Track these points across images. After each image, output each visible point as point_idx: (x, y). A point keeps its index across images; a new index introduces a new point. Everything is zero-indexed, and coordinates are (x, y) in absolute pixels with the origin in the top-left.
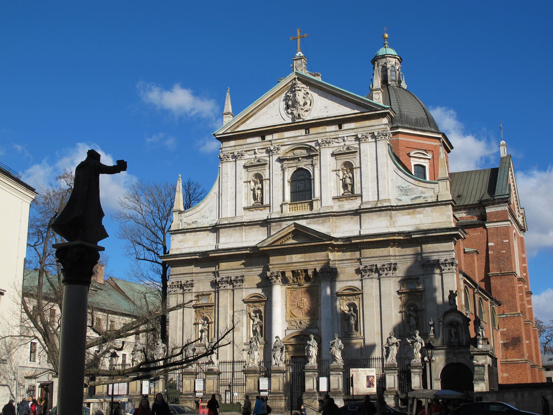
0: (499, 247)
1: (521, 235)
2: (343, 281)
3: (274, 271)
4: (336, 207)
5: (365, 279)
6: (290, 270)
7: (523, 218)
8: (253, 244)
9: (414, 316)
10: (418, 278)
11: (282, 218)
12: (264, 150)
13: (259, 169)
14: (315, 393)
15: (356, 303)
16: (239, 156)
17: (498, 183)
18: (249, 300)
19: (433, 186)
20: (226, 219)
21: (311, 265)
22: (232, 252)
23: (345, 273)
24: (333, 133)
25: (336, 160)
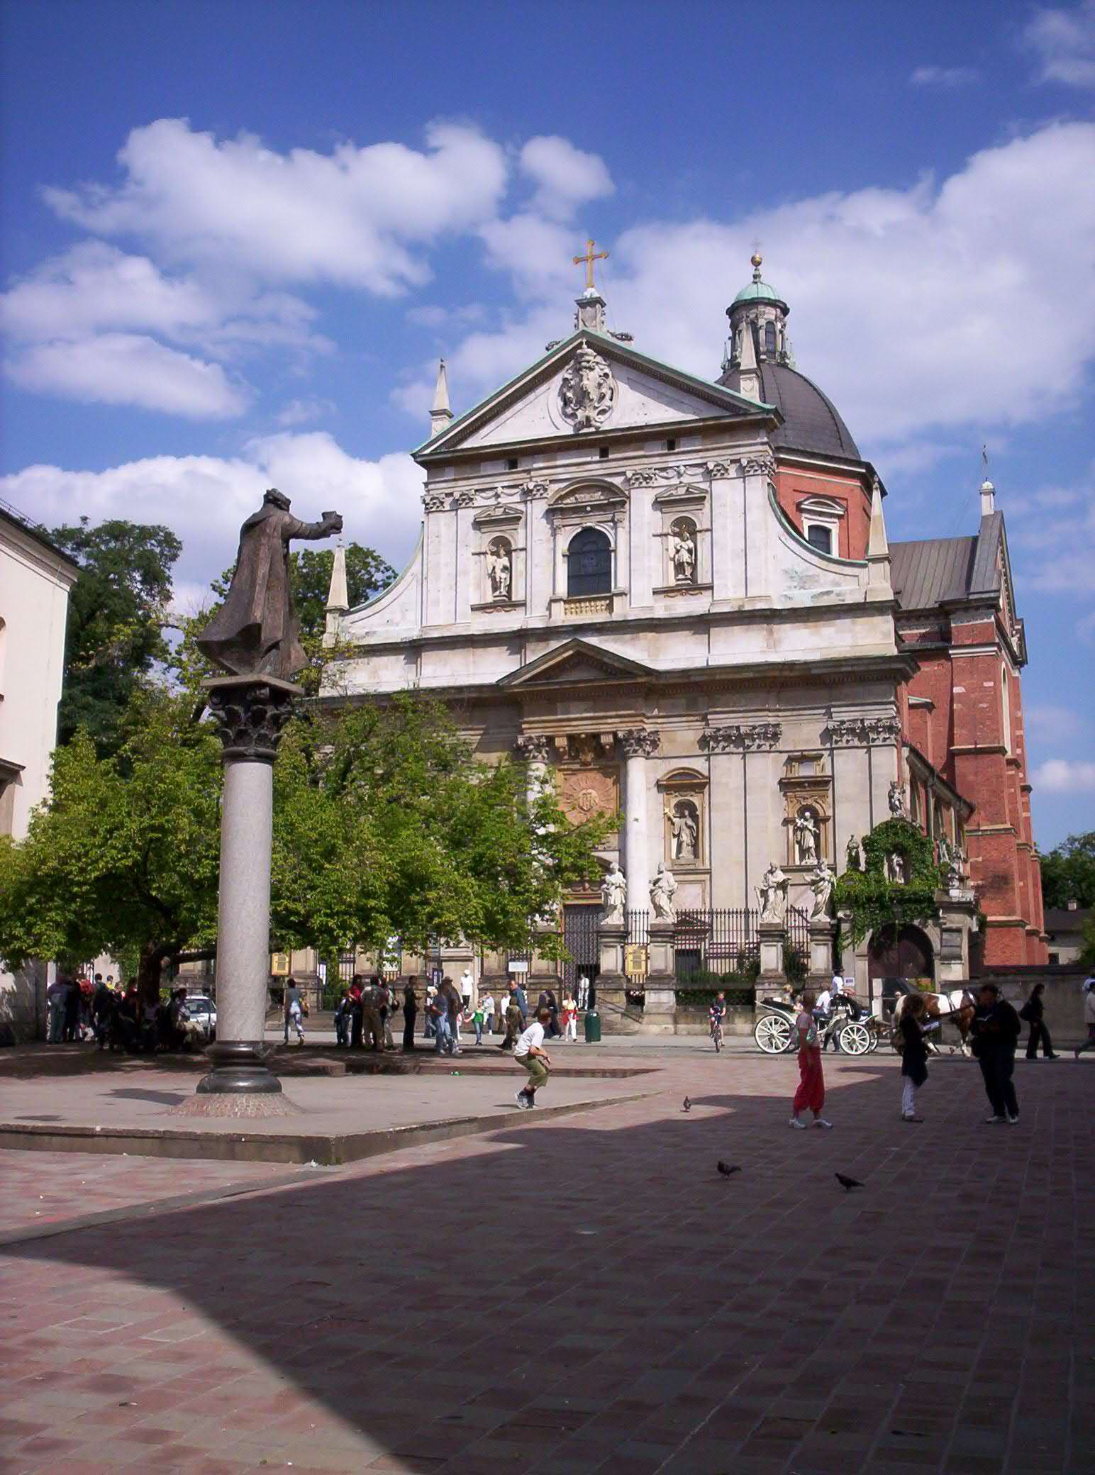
0: (973, 696)
1: (1016, 674)
3: (533, 735)
4: (662, 608)
7: (1020, 639)
8: (492, 680)
9: (810, 830)
10: (820, 757)
12: (516, 490)
13: (503, 528)
14: (619, 977)
15: (696, 800)
16: (464, 500)
17: (976, 567)
24: (657, 459)
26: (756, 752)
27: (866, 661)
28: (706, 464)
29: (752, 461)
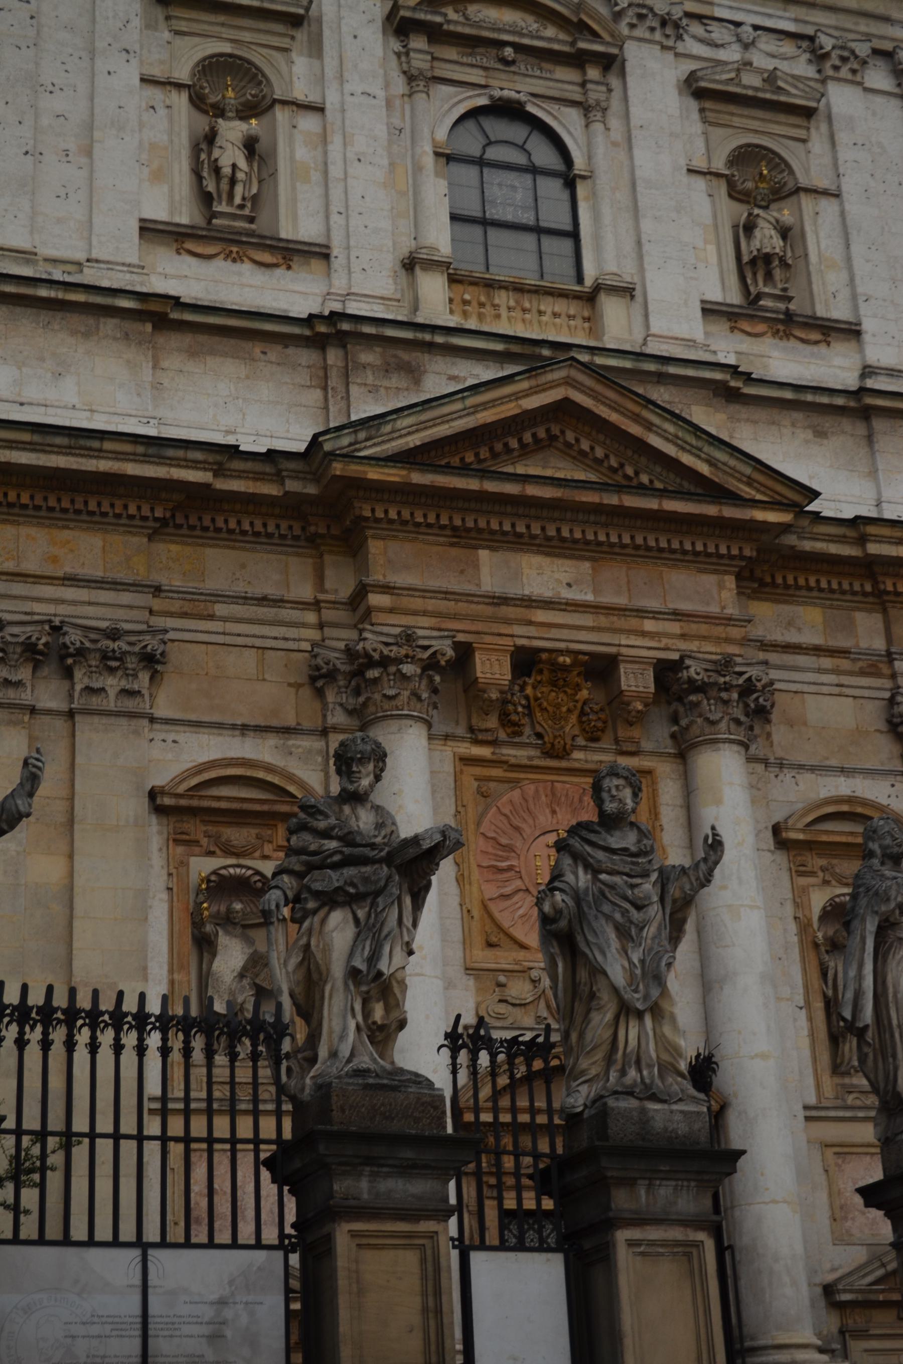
2: (801, 767)
6: (508, 641)
11: (434, 329)
13: (247, 36)
18: (195, 803)
20: (26, 255)
21: (644, 634)
22: (100, 453)
23: (805, 724)
25: (704, 121)
28: (811, 39)
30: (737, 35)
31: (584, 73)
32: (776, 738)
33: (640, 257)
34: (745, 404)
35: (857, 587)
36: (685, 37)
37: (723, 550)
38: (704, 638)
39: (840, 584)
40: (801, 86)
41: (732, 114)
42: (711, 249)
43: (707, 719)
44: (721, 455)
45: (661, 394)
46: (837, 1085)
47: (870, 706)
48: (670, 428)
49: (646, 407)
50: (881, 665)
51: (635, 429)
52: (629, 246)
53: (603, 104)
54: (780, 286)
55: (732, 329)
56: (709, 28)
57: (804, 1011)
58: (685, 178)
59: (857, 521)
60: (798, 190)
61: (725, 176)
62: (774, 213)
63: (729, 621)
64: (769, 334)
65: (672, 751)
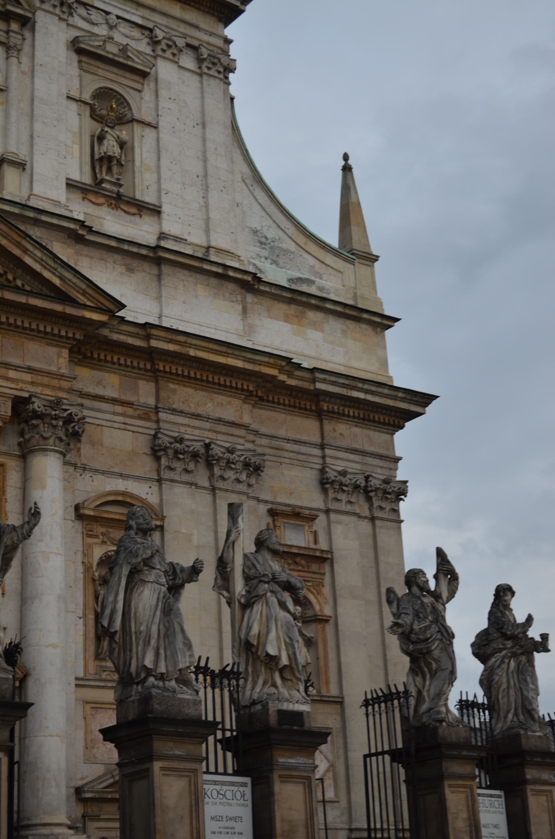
2: (96, 471)
5: (172, 481)
10: (312, 519)
19: (340, 264)
21: (8, 379)
23: (102, 445)
25: (81, 68)
26: (233, 492)
27: (386, 391)
28: (151, 30)
29: (215, 57)
30: (106, 20)
31: (9, 25)
32: (83, 451)
33: (32, 145)
34: (87, 245)
35: (142, 365)
36: (75, 15)
37: (63, 333)
38: (46, 386)
39: (132, 362)
40: (142, 58)
41: (98, 67)
42: (76, 147)
43: (42, 436)
44: (68, 275)
45: (35, 232)
46: (97, 666)
47: (142, 438)
48: (39, 254)
49: (25, 239)
50: (151, 414)
51: (16, 252)
52: (25, 137)
53: (19, 47)
54: (116, 176)
55: (84, 199)
56: (89, 12)
57: (82, 620)
58: (65, 102)
59: (146, 325)
60: (133, 120)
61: (90, 104)
62: (117, 132)
63: (62, 377)
64: (106, 205)
65: (17, 453)
